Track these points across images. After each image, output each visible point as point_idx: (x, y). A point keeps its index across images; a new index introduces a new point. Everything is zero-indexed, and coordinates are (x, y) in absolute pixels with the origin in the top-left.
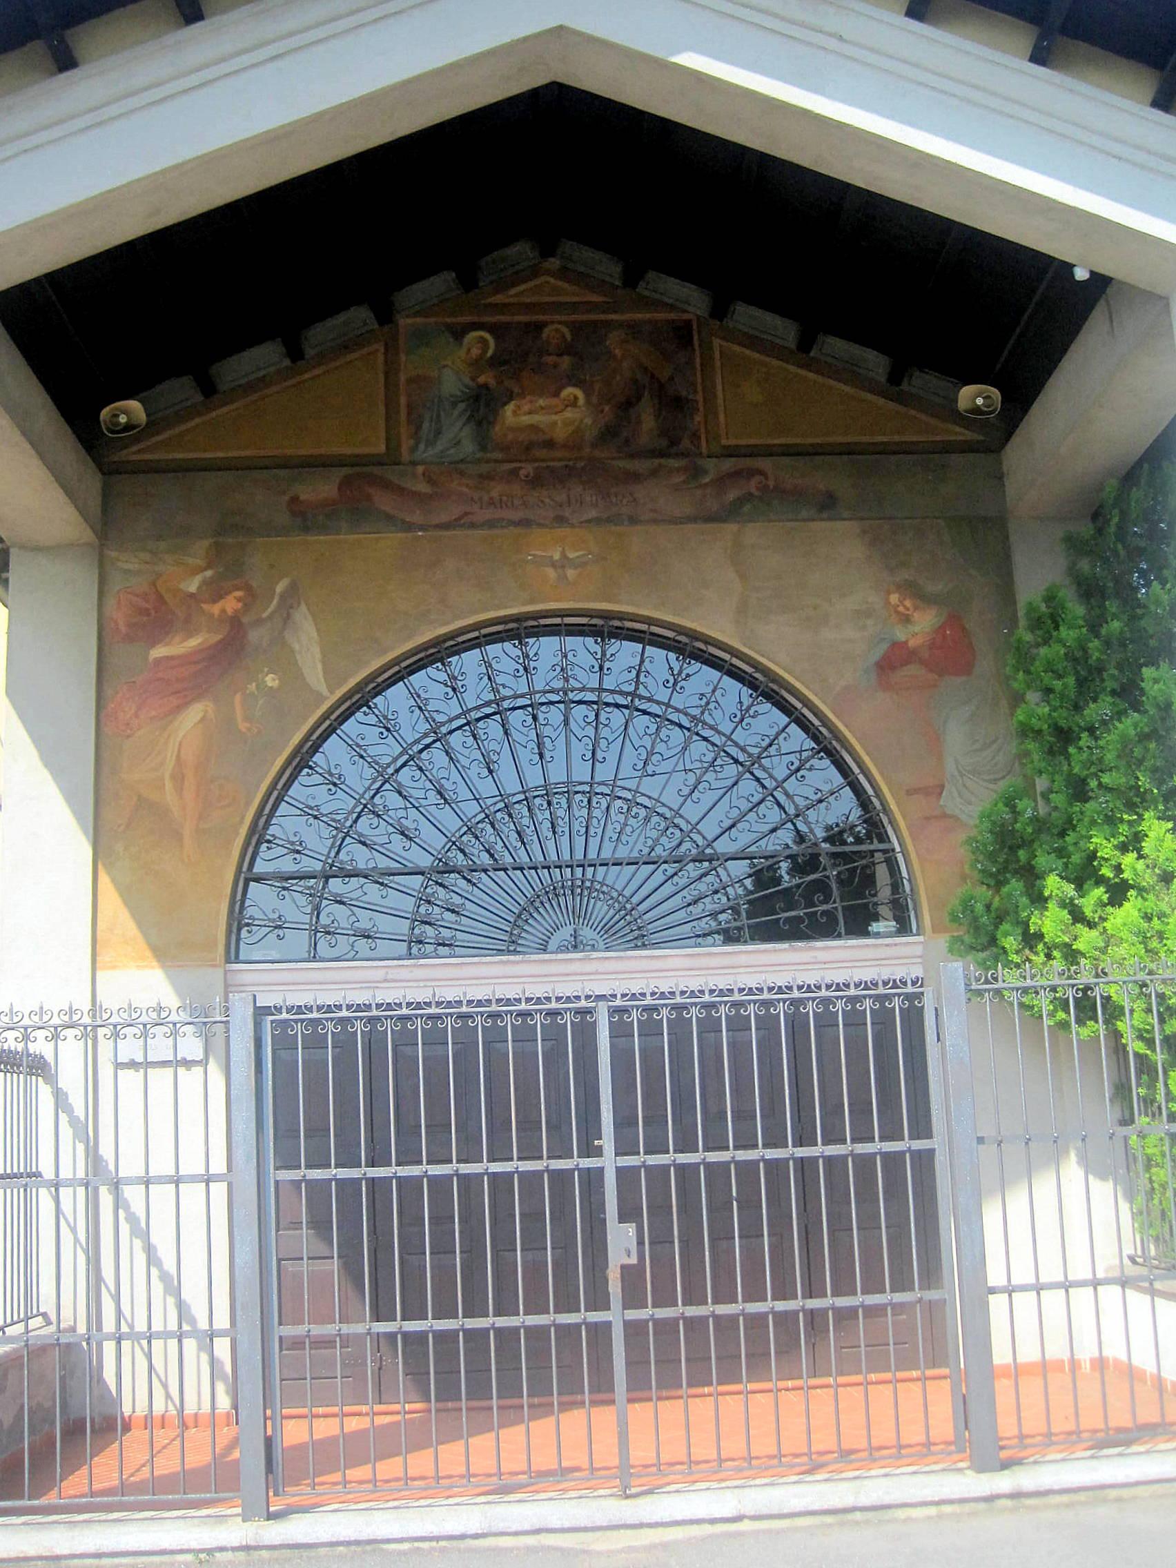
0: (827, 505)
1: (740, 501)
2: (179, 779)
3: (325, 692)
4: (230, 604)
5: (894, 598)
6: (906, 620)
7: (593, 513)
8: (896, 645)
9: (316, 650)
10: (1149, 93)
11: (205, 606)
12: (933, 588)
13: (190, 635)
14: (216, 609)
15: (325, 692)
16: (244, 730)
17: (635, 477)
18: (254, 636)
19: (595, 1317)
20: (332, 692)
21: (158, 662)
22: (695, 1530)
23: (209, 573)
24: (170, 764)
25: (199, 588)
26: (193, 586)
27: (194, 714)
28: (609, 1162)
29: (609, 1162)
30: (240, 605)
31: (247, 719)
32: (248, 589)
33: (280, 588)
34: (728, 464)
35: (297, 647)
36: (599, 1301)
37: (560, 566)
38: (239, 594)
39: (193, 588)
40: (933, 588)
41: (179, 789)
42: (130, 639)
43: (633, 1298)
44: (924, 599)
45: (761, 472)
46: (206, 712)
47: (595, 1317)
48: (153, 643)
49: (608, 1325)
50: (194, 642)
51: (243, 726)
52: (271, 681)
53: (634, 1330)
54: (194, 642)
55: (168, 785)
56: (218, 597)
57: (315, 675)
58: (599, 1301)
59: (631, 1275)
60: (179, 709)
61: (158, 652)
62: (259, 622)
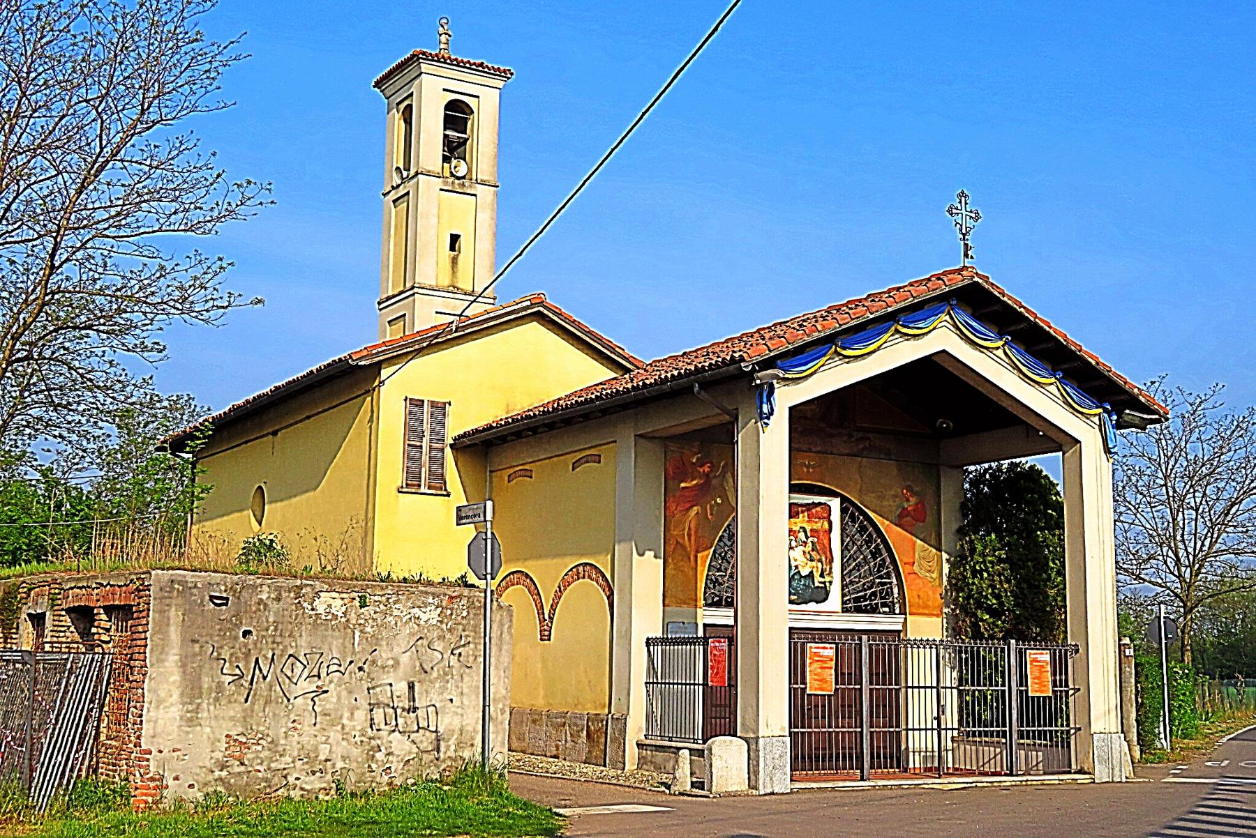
0: (888, 455)
1: (863, 449)
7: (819, 449)
8: (904, 509)
12: (917, 489)
17: (832, 436)
18: (714, 482)
21: (684, 488)
31: (711, 514)
32: (711, 463)
34: (860, 435)
37: (808, 467)
40: (917, 489)
41: (689, 539)
42: (674, 478)
44: (914, 494)
45: (869, 439)
61: (683, 485)
62: (715, 477)
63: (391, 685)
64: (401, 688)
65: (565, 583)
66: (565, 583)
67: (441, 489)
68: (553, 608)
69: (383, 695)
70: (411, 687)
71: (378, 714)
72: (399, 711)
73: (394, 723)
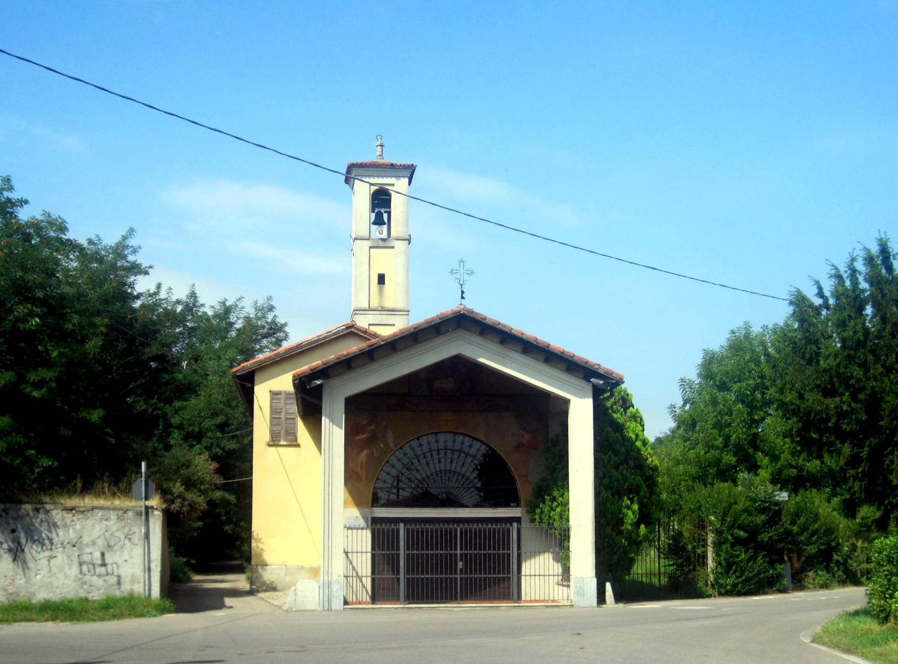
2: (361, 468)
3: (393, 447)
4: (373, 427)
5: (521, 431)
6: (523, 436)
10: (564, 368)
13: (364, 433)
14: (369, 428)
15: (393, 447)
19: (456, 576)
21: (359, 440)
22: (470, 608)
24: (360, 462)
26: (364, 422)
27: (364, 453)
28: (459, 552)
29: (459, 552)
36: (456, 573)
43: (461, 573)
47: (456, 576)
49: (457, 578)
50: (365, 436)
52: (382, 445)
53: (461, 579)
54: (365, 436)
55: (359, 469)
56: (370, 425)
57: (391, 444)
58: (456, 573)
59: (461, 570)
60: (361, 451)
61: (357, 438)
63: (91, 553)
64: (97, 555)
67: (294, 441)
69: (87, 558)
70: (103, 554)
71: (85, 568)
72: (96, 566)
73: (93, 571)
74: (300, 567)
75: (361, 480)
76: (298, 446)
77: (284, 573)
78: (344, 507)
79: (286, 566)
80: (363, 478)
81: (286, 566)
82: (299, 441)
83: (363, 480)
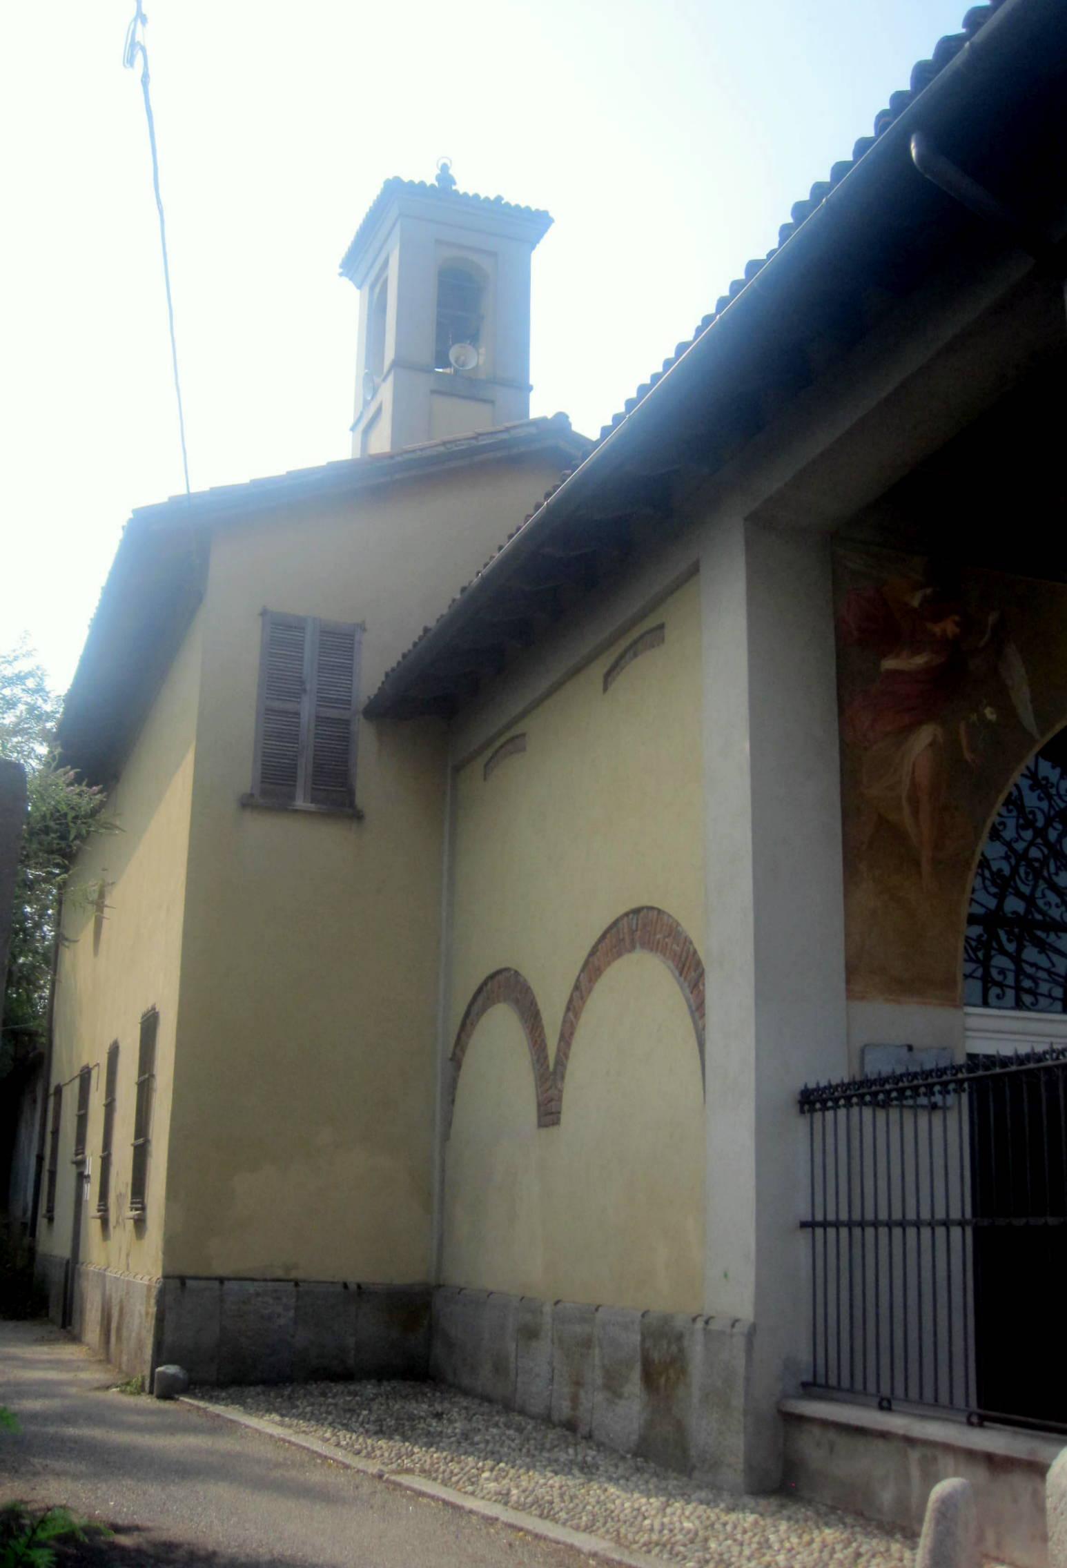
4: (949, 627)
9: (1026, 689)
11: (929, 626)
13: (917, 651)
14: (937, 629)
16: (970, 760)
20: (1043, 734)
21: (894, 674)
23: (929, 591)
25: (921, 605)
30: (957, 630)
33: (992, 618)
35: (1009, 682)
38: (957, 618)
39: (915, 603)
41: (915, 813)
46: (935, 736)
48: (884, 655)
50: (920, 660)
51: (968, 756)
52: (990, 714)
54: (920, 660)
60: (909, 729)
61: (889, 664)
65: (592, 970)
66: (592, 970)
68: (566, 1038)
74: (353, 1287)
75: (917, 864)
76: (357, 816)
77: (291, 1313)
78: (851, 995)
79: (297, 1284)
80: (926, 855)
81: (297, 1284)
82: (361, 799)
83: (926, 855)
